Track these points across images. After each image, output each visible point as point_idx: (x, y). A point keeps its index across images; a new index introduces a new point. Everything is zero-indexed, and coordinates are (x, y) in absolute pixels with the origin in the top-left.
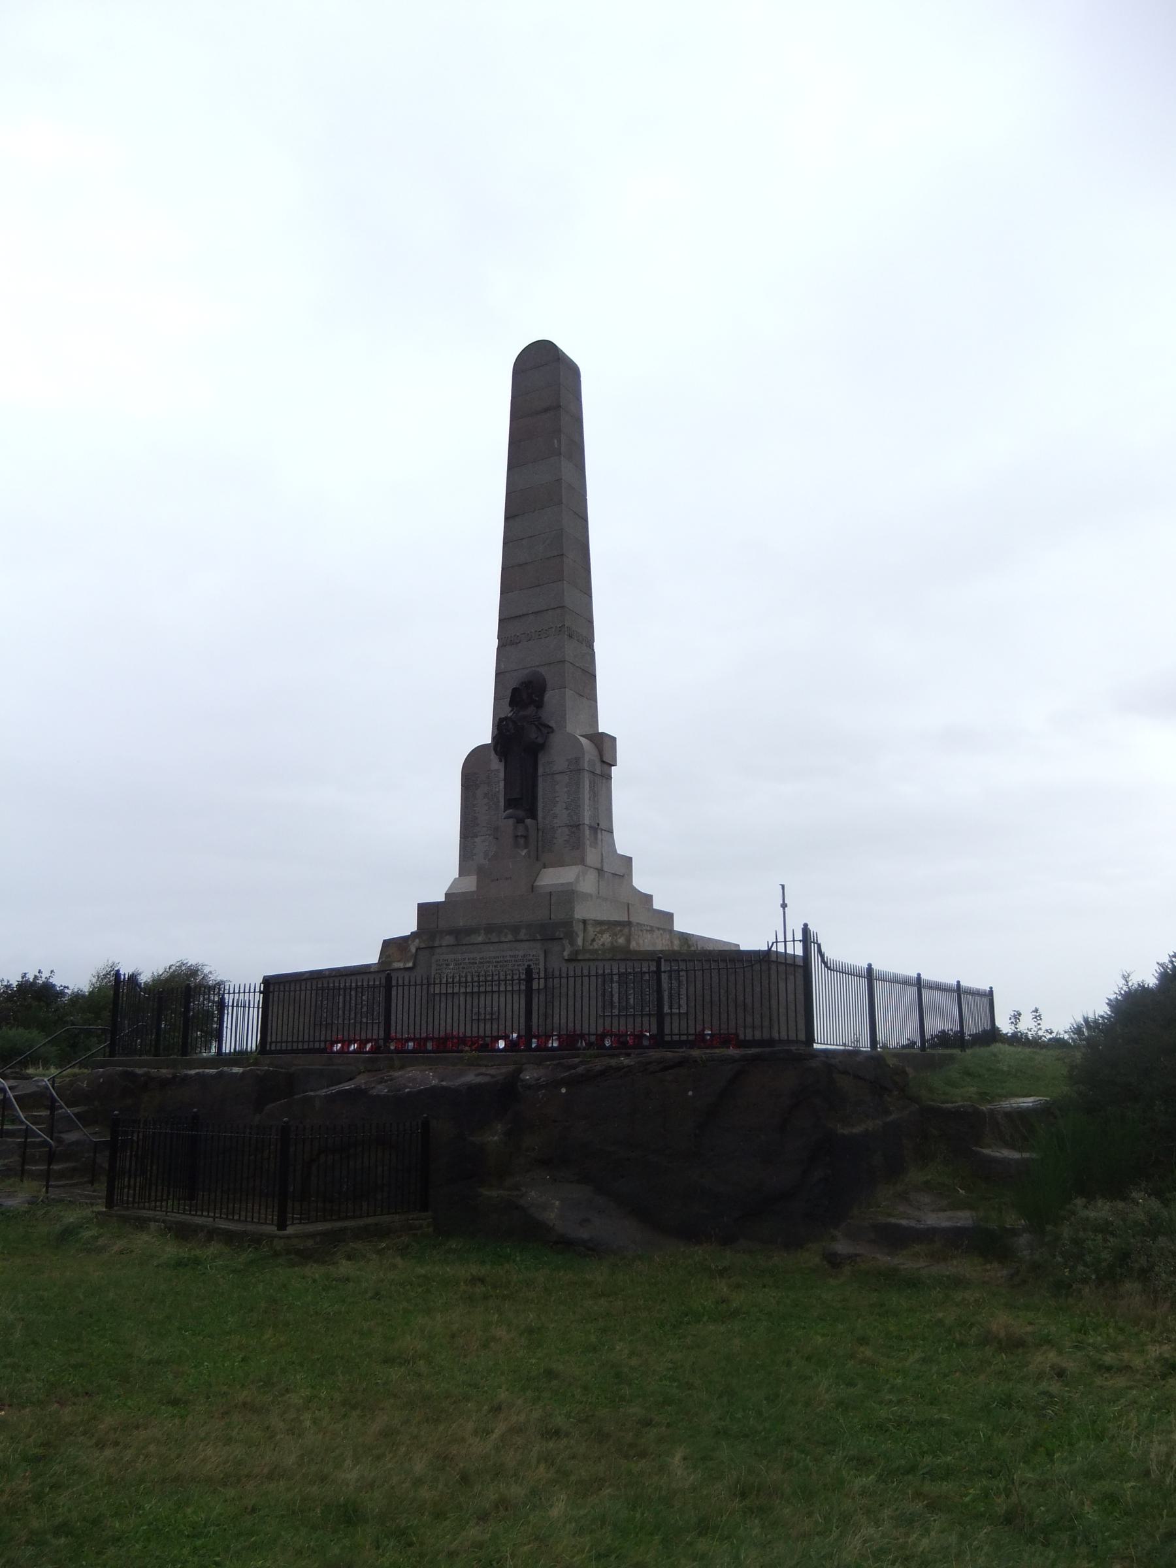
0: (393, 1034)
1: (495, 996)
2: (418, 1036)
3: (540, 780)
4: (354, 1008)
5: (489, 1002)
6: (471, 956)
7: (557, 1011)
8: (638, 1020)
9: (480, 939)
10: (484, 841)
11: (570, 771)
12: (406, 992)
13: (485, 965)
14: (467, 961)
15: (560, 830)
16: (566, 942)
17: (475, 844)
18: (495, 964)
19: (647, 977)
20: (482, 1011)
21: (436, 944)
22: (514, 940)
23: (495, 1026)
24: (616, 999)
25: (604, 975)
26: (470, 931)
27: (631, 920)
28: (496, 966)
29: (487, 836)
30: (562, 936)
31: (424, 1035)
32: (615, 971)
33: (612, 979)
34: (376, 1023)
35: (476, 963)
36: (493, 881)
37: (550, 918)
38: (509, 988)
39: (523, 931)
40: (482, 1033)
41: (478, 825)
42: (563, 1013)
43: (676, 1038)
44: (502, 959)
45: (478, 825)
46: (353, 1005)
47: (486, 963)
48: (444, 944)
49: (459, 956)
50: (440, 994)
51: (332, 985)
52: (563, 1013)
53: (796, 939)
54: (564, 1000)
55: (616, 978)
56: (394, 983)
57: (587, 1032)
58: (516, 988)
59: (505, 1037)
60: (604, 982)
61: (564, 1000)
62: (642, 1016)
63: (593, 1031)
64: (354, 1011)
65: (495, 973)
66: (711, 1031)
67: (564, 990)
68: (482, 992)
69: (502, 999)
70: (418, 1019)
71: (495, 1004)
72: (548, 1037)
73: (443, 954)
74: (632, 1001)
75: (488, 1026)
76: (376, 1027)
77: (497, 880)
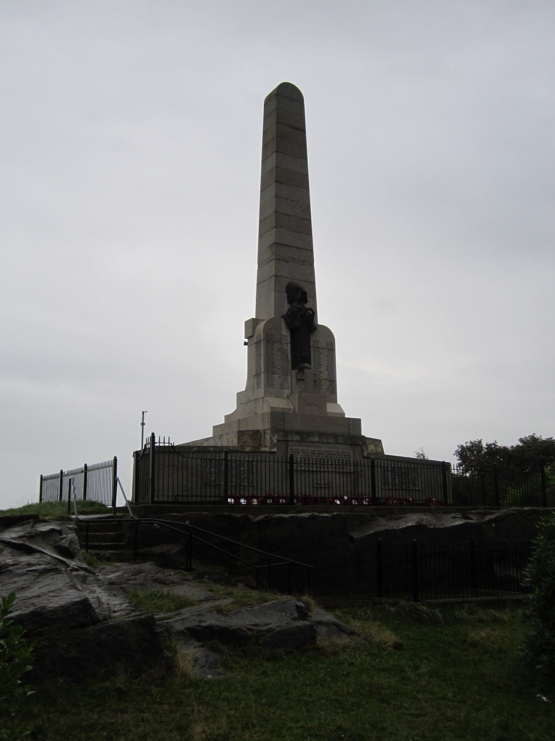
0: (295, 494)
1: (326, 474)
2: (285, 495)
3: (312, 349)
4: (235, 475)
5: (322, 477)
6: (313, 449)
7: (360, 485)
8: (391, 492)
9: (316, 439)
10: (279, 377)
11: (328, 349)
12: (276, 466)
13: (321, 455)
14: (310, 451)
15: (323, 382)
16: (364, 447)
17: (274, 378)
18: (326, 455)
19: (403, 470)
20: (319, 482)
21: (290, 438)
22: (335, 442)
23: (327, 492)
24: (390, 479)
25: (384, 467)
26: (310, 434)
27: (144, 422)
28: (327, 457)
29: (281, 375)
30: (361, 443)
31: (276, 495)
32: (389, 466)
33: (388, 469)
34: (251, 486)
35: (315, 454)
36: (308, 405)
37: (349, 433)
38: (334, 470)
39: (340, 438)
40: (323, 495)
41: (275, 366)
42: (363, 486)
43: (418, 502)
44: (330, 453)
45: (275, 366)
46: (234, 473)
47: (321, 454)
48: (295, 439)
49: (305, 448)
50: (332, 472)
51: (407, 466)
52: (363, 486)
53: (165, 442)
54: (363, 479)
55: (390, 469)
56: (376, 465)
57: (328, 496)
58: (337, 470)
59: (341, 499)
60: (384, 472)
61: (363, 479)
62: (402, 490)
63: (384, 497)
64: (235, 477)
65: (321, 460)
66: (435, 499)
67: (363, 474)
68: (303, 471)
69: (330, 476)
70: (280, 485)
71: (326, 478)
72: (364, 499)
73: (294, 445)
74: (397, 482)
75: (323, 491)
76: (251, 489)
77: (310, 405)
